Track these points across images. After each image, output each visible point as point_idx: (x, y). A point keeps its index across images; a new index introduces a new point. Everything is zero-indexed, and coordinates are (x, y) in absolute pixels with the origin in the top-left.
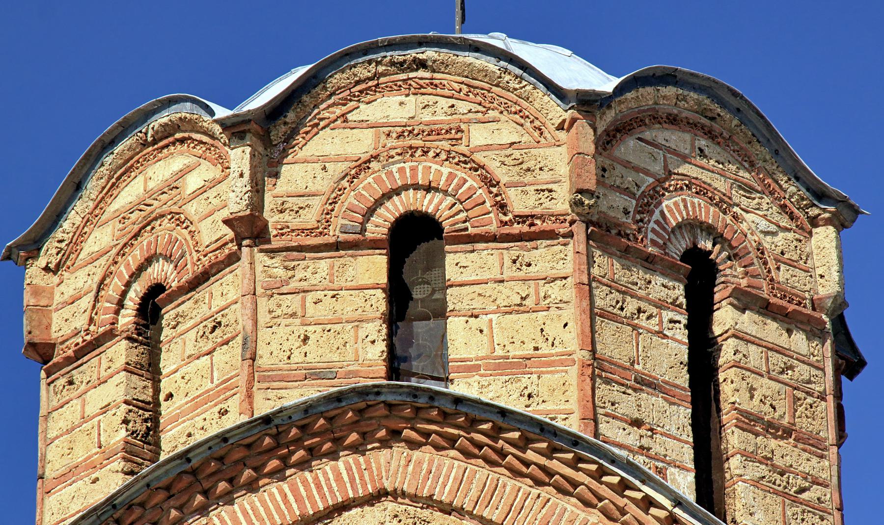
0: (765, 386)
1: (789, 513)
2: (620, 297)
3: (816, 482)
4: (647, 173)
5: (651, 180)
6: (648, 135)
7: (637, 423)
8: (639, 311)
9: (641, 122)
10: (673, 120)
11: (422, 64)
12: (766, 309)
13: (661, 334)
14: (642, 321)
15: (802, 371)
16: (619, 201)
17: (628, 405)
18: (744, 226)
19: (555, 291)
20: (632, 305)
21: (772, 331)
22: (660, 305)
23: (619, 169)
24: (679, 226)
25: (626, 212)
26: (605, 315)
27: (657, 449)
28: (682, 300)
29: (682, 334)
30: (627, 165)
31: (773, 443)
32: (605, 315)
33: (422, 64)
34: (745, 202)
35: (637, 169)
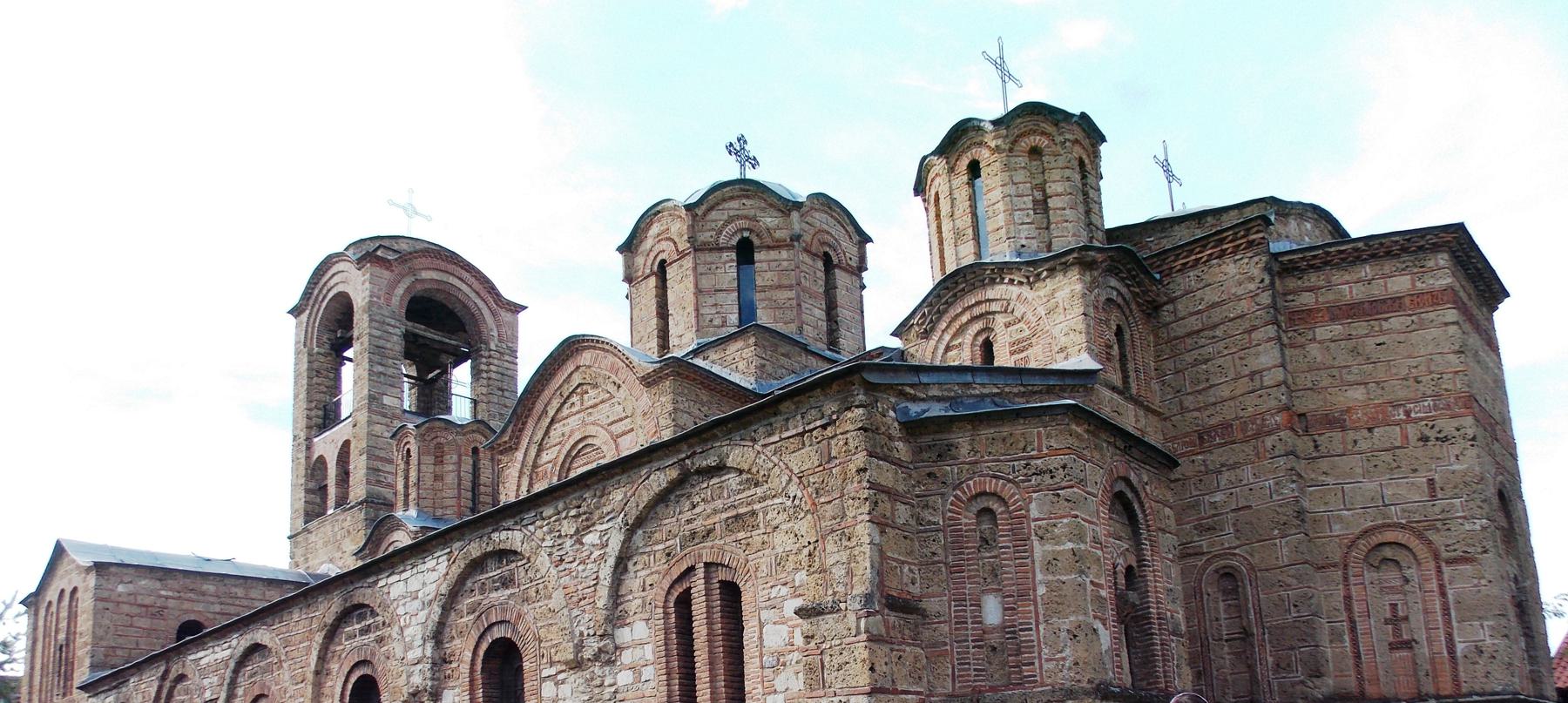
0: (769, 275)
1: (777, 313)
2: (709, 266)
3: (790, 299)
4: (720, 220)
5: (722, 222)
6: (721, 208)
7: (716, 305)
8: (717, 268)
9: (718, 204)
10: (732, 198)
11: (659, 212)
12: (769, 248)
13: (725, 273)
14: (719, 270)
15: (785, 264)
16: (709, 234)
17: (711, 301)
18: (761, 223)
19: (688, 272)
20: (714, 267)
21: (773, 254)
22: (725, 263)
23: (709, 223)
24: (736, 232)
25: (712, 237)
26: (701, 274)
27: (722, 310)
28: (735, 258)
29: (734, 270)
30: (712, 221)
31: (772, 292)
32: (701, 274)
33: (659, 212)
34: (762, 215)
35: (716, 221)
